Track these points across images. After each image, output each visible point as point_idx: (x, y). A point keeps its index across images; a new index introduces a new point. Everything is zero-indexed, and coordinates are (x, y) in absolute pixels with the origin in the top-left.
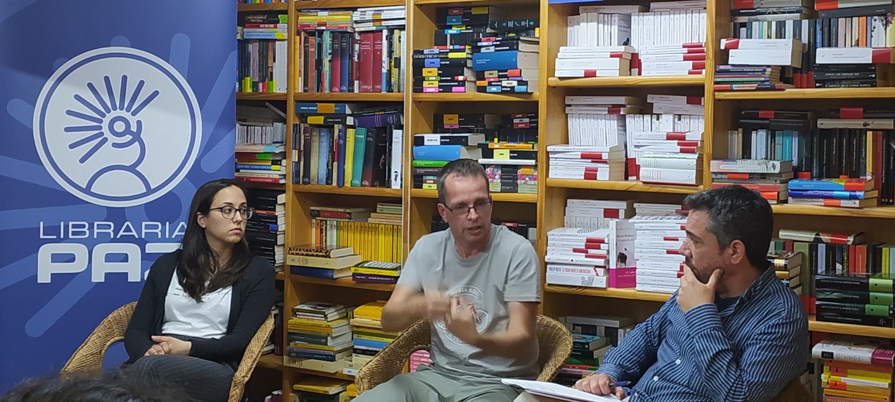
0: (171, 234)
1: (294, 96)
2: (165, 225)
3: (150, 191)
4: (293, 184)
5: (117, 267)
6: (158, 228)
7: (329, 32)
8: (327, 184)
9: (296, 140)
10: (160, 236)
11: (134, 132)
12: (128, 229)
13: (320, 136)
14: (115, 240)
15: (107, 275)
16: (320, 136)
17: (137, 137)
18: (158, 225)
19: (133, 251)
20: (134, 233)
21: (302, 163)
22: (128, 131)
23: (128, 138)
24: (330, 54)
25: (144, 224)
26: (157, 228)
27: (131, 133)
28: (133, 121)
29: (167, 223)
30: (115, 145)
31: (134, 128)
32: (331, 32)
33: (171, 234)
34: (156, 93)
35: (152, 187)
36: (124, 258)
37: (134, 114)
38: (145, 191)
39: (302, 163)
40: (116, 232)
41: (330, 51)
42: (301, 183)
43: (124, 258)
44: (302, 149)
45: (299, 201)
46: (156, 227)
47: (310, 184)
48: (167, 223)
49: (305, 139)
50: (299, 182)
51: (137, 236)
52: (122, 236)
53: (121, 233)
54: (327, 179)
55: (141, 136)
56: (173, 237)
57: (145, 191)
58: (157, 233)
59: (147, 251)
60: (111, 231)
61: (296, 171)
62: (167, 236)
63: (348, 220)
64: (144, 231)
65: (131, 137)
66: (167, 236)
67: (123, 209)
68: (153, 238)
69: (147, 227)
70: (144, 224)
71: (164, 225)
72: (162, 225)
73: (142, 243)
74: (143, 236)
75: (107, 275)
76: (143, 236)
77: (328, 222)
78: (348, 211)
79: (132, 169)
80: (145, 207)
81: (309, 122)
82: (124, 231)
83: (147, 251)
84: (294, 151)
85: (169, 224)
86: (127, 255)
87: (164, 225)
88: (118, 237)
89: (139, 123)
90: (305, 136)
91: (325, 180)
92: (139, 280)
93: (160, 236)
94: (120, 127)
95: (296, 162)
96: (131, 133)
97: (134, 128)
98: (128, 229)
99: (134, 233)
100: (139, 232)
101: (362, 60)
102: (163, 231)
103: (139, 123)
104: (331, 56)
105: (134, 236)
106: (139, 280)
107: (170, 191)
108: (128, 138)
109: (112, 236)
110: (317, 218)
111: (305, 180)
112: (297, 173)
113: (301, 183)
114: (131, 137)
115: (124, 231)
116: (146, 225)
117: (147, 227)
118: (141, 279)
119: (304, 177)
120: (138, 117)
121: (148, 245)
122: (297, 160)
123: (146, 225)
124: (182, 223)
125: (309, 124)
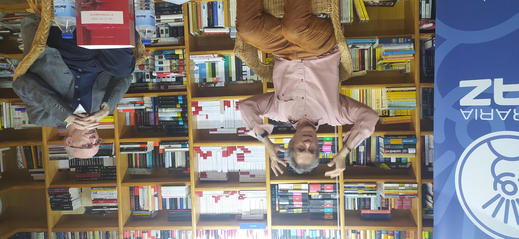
0: (474, 113)
2: (477, 118)
3: (488, 141)
10: (481, 110)
12: (503, 115)
14: (513, 107)
17: (497, 179)
19: (500, 100)
20: (499, 112)
22: (504, 184)
23: (503, 179)
25: (492, 119)
26: (483, 115)
27: (501, 182)
28: (500, 191)
29: (476, 119)
31: (499, 186)
33: (474, 113)
36: (506, 95)
37: (499, 196)
38: (491, 142)
40: (512, 113)
43: (506, 95)
46: (484, 116)
48: (476, 119)
51: (497, 110)
52: (508, 111)
53: (508, 113)
55: (494, 179)
57: (491, 142)
58: (483, 112)
62: (476, 110)
64: (492, 114)
65: (501, 179)
66: (476, 110)
67: (507, 130)
68: (486, 109)
69: (490, 117)
70: (492, 119)
71: (479, 118)
72: (480, 118)
73: (494, 105)
74: (492, 110)
76: (492, 110)
79: (500, 157)
82: (506, 113)
85: (475, 118)
87: (479, 118)
88: (510, 110)
89: (495, 188)
93: (481, 110)
96: (501, 182)
97: (499, 186)
98: (503, 115)
99: (499, 112)
100: (495, 114)
102: (479, 113)
103: (495, 188)
106: (495, 79)
108: (503, 179)
109: (515, 110)
114: (501, 179)
115: (506, 113)
117: (490, 117)
118: (494, 81)
120: (495, 193)
124: (467, 119)
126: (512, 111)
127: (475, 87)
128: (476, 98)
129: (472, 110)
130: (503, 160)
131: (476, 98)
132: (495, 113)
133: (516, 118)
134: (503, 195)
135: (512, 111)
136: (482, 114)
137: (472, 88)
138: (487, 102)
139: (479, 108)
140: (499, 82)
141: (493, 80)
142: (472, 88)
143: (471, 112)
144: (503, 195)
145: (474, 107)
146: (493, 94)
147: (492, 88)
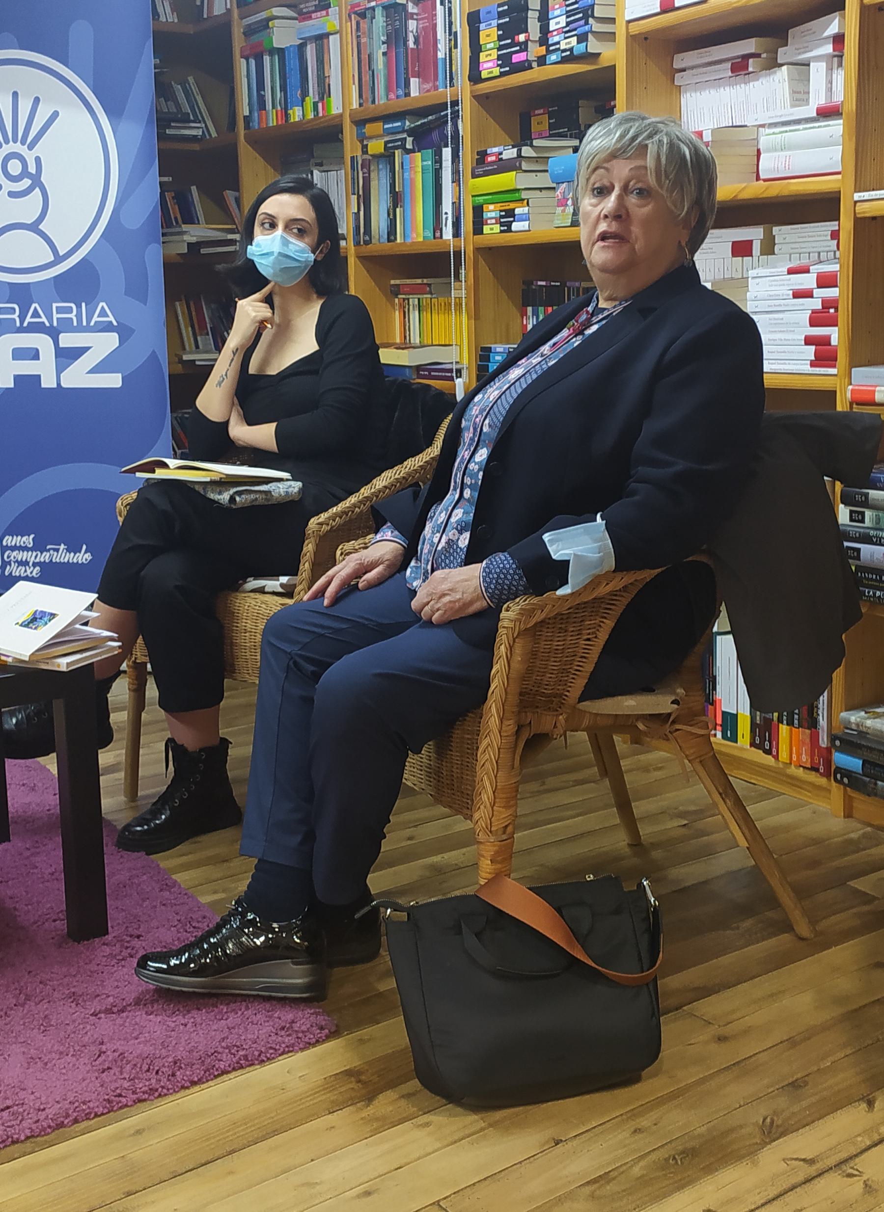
0: (89, 320)
1: (350, 116)
3: (59, 259)
4: (354, 246)
5: (27, 368)
6: (71, 312)
7: (380, 8)
8: (389, 240)
9: (354, 180)
10: (75, 324)
11: (32, 174)
12: (36, 314)
13: (379, 170)
14: (21, 330)
15: (18, 378)
16: (379, 170)
17: (37, 182)
18: (71, 308)
19: (42, 342)
20: (44, 319)
21: (362, 213)
22: (25, 173)
23: (26, 183)
24: (384, 43)
25: (55, 305)
29: (83, 305)
30: (12, 194)
31: (32, 169)
32: (383, 7)
33: (89, 318)
34: (55, 115)
35: (61, 254)
36: (35, 355)
37: (31, 147)
38: (52, 259)
39: (362, 213)
40: (22, 318)
41: (383, 38)
42: (362, 243)
43: (35, 355)
44: (361, 193)
45: (368, 271)
46: (70, 310)
47: (371, 243)
48: (83, 305)
49: (364, 178)
50: (360, 242)
51: (47, 324)
52: (29, 323)
53: (28, 319)
54: (389, 234)
55: (42, 179)
56: (92, 324)
57: (52, 259)
59: (61, 345)
60: (16, 316)
61: (356, 226)
62: (84, 323)
63: (429, 296)
64: (55, 316)
65: (30, 182)
66: (84, 323)
68: (67, 326)
71: (79, 307)
73: (54, 333)
74: (55, 324)
75: (18, 378)
76: (55, 324)
77: (411, 300)
78: (425, 281)
79: (34, 227)
80: (55, 282)
81: (370, 152)
83: (61, 345)
84: (353, 196)
85: (86, 305)
86: (37, 350)
87: (79, 307)
89: (38, 160)
90: (363, 173)
91: (386, 236)
92: (55, 386)
93: (75, 324)
94: (15, 167)
95: (355, 213)
97: (32, 169)
99: (44, 319)
100: (50, 317)
101: (421, 46)
102: (79, 316)
103: (38, 160)
104: (386, 45)
105: (43, 323)
106: (55, 386)
107: (83, 258)
108: (26, 183)
109: (18, 324)
110: (400, 296)
111: (365, 239)
112: (357, 228)
113: (362, 243)
114: (30, 182)
116: (57, 307)
117: (59, 310)
119: (365, 233)
120: (38, 150)
121: (61, 336)
122: (356, 211)
123: (57, 307)
125: (371, 155)
126: (22, 322)
127: (91, 371)
128: (85, 349)
129: (92, 324)
130: (29, 222)
131: (85, 349)
132: (50, 319)
133: (14, 309)
134: (22, 150)
135: (22, 322)
136: (73, 316)
137: (96, 370)
138: (67, 340)
139: (80, 329)
140: (48, 382)
141: (59, 384)
142: (96, 370)
143: (95, 318)
144: (22, 150)
145: (88, 329)
146: (57, 356)
147: (59, 370)
